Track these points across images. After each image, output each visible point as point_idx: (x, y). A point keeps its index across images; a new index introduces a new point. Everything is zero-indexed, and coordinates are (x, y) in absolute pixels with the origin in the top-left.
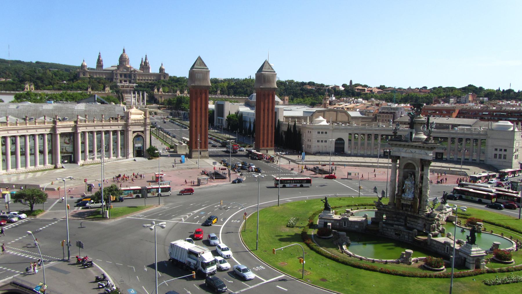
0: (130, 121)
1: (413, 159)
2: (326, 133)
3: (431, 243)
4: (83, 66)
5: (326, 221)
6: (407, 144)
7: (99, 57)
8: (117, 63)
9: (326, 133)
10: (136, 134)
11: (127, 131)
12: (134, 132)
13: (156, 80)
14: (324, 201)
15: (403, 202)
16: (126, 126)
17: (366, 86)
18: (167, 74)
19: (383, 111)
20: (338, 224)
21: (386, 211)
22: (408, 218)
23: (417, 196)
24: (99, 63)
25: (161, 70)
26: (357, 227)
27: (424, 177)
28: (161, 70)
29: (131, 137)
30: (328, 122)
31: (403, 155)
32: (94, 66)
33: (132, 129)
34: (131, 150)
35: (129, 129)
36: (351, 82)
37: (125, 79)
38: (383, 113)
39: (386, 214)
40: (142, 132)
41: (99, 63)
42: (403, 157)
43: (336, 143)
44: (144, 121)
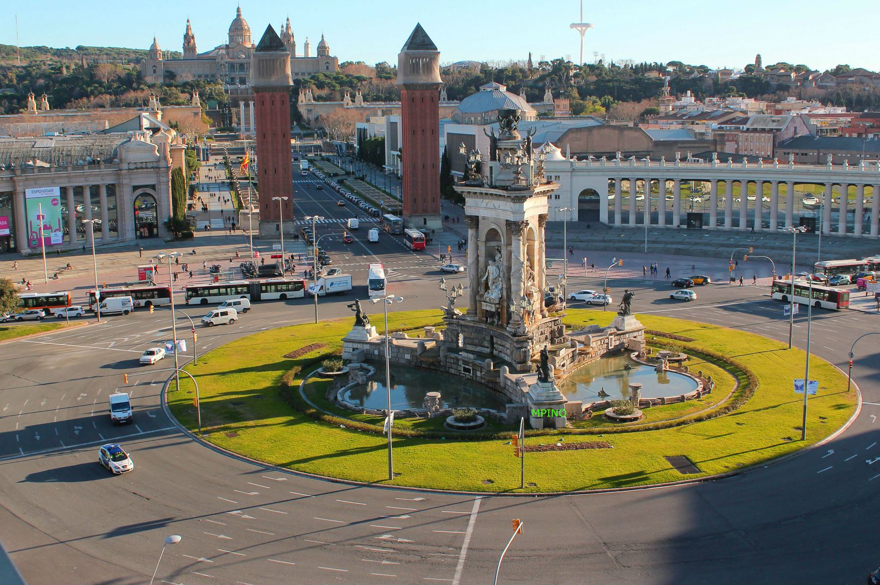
0: (125, 166)
1: (496, 221)
2: (558, 177)
3: (506, 384)
4: (154, 51)
5: (355, 346)
6: (483, 190)
7: (188, 28)
8: (225, 40)
9: (558, 177)
10: (139, 192)
11: (120, 185)
12: (135, 188)
13: (309, 74)
14: (354, 307)
15: (484, 308)
16: (118, 174)
17: (799, 68)
18: (335, 59)
19: (755, 127)
20: (376, 352)
21: (461, 325)
22: (495, 340)
23: (505, 294)
24: (188, 38)
25: (322, 48)
26: (408, 357)
27: (513, 257)
28: (322, 48)
29: (127, 197)
30: (564, 154)
31: (481, 213)
32: (178, 47)
33: (128, 182)
34: (129, 225)
35: (125, 181)
36: (758, 58)
37: (242, 74)
38: (755, 130)
39: (463, 331)
40: (153, 187)
41: (188, 38)
42: (484, 218)
43: (580, 201)
44: (155, 165)
